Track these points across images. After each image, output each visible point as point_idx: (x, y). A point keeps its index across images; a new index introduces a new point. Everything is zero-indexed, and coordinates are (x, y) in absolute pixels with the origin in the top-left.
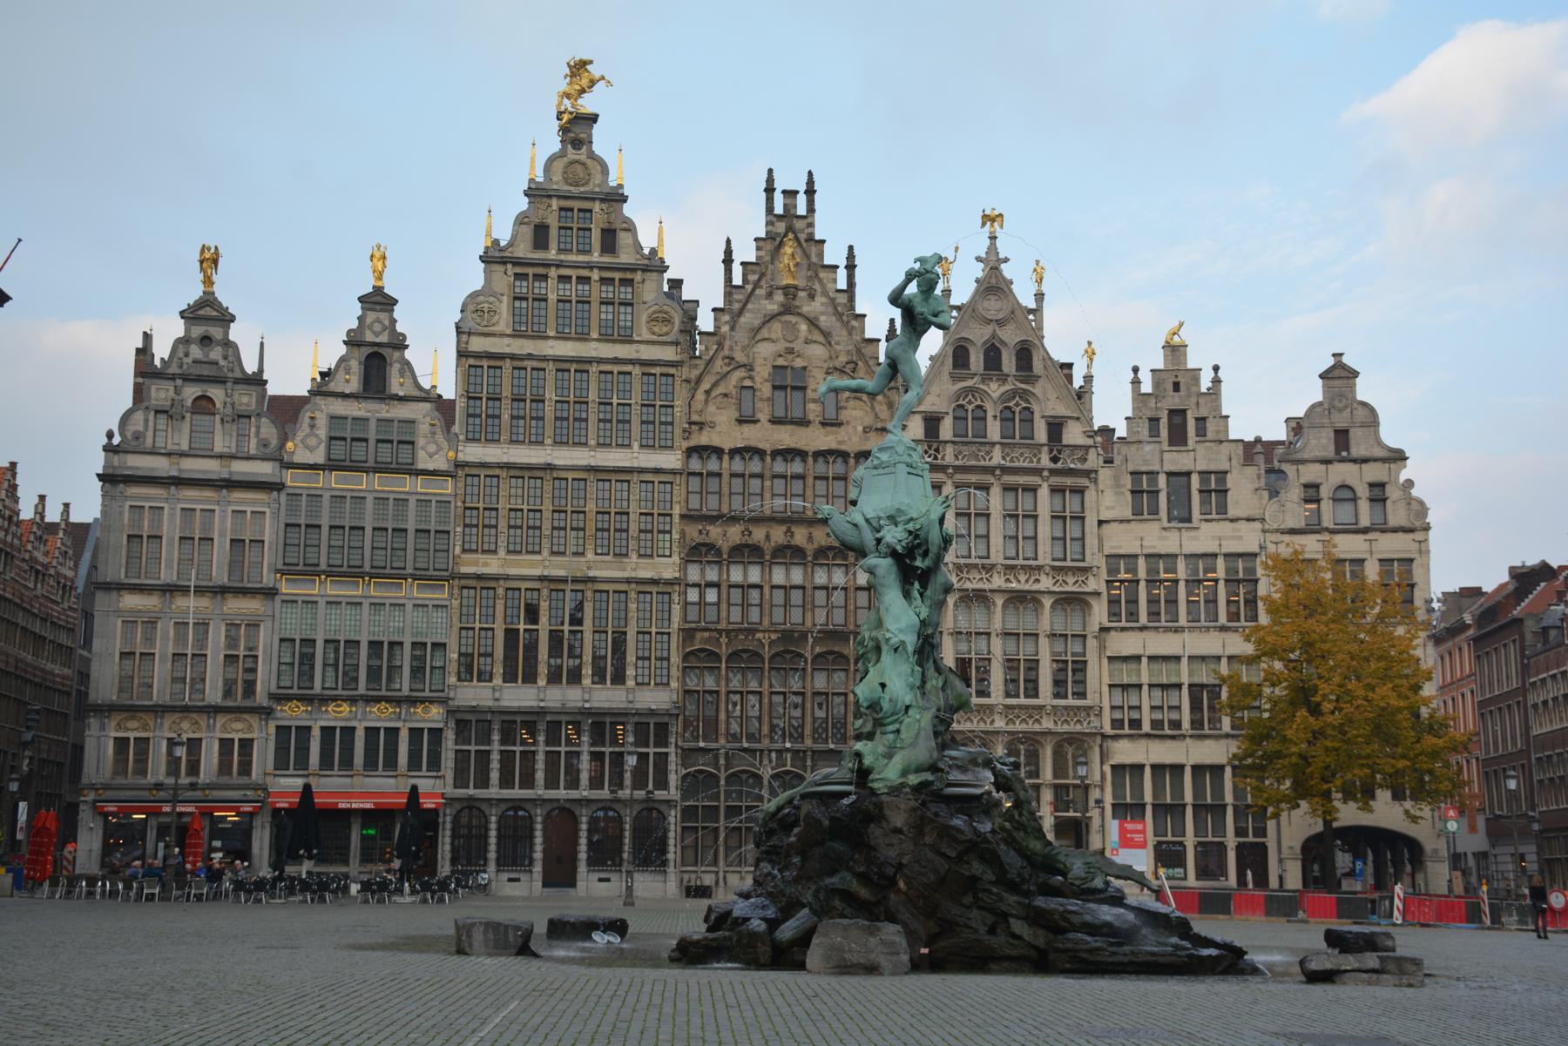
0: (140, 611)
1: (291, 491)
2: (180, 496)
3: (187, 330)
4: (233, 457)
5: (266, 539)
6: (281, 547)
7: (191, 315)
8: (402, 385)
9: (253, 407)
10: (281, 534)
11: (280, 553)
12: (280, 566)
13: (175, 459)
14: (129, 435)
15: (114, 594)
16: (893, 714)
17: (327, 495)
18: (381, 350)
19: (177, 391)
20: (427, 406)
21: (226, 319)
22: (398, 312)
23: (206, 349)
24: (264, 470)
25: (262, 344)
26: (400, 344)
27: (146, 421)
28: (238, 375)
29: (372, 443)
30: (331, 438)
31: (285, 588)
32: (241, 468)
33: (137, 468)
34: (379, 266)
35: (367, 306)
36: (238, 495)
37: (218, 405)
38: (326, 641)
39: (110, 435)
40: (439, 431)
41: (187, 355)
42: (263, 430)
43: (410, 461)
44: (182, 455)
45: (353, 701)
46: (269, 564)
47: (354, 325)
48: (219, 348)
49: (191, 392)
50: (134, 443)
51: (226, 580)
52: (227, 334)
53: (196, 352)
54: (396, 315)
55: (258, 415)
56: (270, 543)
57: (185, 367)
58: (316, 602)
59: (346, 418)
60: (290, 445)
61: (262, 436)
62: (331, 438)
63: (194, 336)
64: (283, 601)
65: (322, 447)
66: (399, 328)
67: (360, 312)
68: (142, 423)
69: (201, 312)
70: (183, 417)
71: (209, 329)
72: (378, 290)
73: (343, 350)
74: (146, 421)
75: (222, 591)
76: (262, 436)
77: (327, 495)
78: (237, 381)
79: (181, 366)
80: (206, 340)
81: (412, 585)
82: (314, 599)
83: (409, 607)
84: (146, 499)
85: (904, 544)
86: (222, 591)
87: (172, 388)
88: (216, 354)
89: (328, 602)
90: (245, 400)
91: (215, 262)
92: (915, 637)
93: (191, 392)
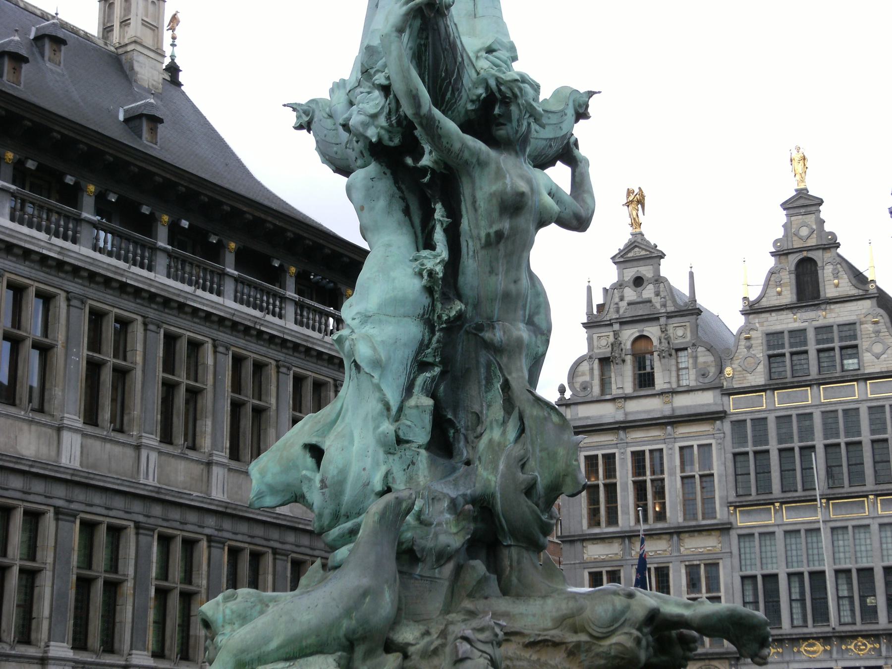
0: (603, 561)
1: (734, 418)
2: (629, 440)
3: (621, 274)
4: (674, 392)
5: (715, 471)
6: (731, 478)
7: (622, 259)
8: (837, 286)
9: (688, 338)
10: (730, 464)
11: (732, 484)
12: (732, 498)
13: (621, 403)
14: (577, 386)
15: (578, 545)
16: (336, 518)
17: (771, 418)
18: (811, 255)
19: (616, 334)
20: (867, 304)
21: (655, 256)
22: (825, 212)
23: (639, 289)
24: (706, 400)
25: (691, 275)
26: (832, 244)
27: (592, 370)
28: (671, 308)
29: (812, 354)
30: (770, 357)
31: (742, 522)
32: (684, 403)
33: (588, 418)
34: (799, 168)
35: (792, 211)
36: (683, 430)
37: (655, 342)
38: (790, 575)
39: (562, 390)
40: (882, 327)
41: (622, 299)
42: (701, 360)
43: (856, 367)
44: (627, 398)
45: (826, 639)
46: (721, 498)
47: (780, 233)
48: (651, 286)
49: (629, 334)
50: (582, 394)
51: (681, 520)
52: (658, 270)
53: (630, 294)
54: (822, 216)
55: (694, 345)
56: (720, 476)
57: (621, 311)
58: (773, 533)
59: (782, 332)
60: (728, 371)
61: (700, 366)
62: (770, 357)
63: (626, 279)
64: (740, 536)
65: (761, 369)
66: (827, 228)
67: (784, 220)
68: (588, 373)
69: (630, 255)
70: (624, 361)
71: (640, 269)
72: (802, 193)
73: (771, 262)
74: (592, 370)
75: (678, 532)
76: (700, 366)
77: (771, 418)
78: (670, 316)
79: (618, 311)
80: (638, 282)
81: (875, 504)
82: (771, 529)
83: (875, 527)
84: (598, 447)
85: (382, 121)
86: (678, 532)
87: (612, 334)
88: (648, 292)
89: (786, 532)
90: (680, 332)
91: (641, 202)
92: (413, 331)
93: (629, 334)
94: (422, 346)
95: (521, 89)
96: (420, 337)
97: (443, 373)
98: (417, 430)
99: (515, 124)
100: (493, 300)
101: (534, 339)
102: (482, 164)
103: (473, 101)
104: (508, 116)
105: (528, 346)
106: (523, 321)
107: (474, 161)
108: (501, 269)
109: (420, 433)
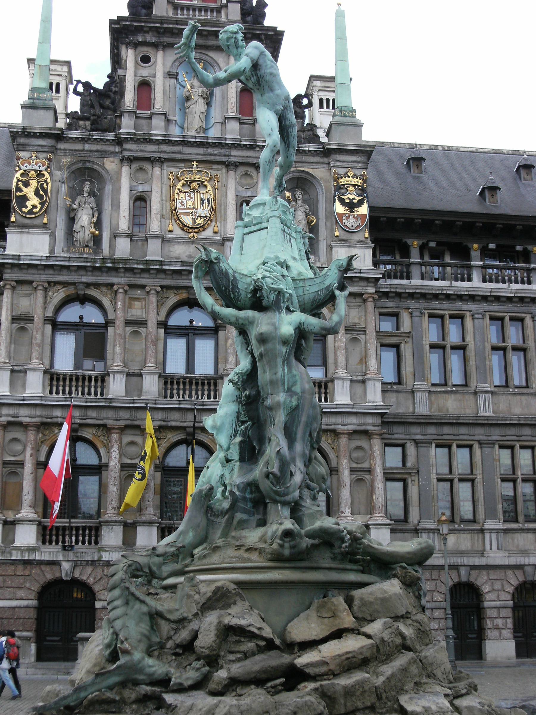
94: (238, 414)
95: (262, 283)
96: (237, 410)
97: (253, 424)
98: (235, 454)
99: (266, 298)
100: (267, 385)
101: (288, 399)
102: (251, 323)
103: (250, 293)
104: (262, 295)
105: (284, 404)
106: (284, 391)
107: (247, 322)
108: (267, 369)
109: (235, 455)
